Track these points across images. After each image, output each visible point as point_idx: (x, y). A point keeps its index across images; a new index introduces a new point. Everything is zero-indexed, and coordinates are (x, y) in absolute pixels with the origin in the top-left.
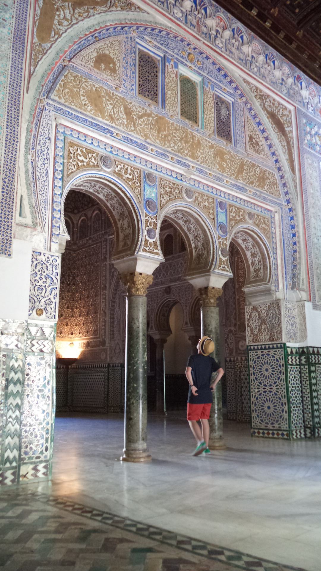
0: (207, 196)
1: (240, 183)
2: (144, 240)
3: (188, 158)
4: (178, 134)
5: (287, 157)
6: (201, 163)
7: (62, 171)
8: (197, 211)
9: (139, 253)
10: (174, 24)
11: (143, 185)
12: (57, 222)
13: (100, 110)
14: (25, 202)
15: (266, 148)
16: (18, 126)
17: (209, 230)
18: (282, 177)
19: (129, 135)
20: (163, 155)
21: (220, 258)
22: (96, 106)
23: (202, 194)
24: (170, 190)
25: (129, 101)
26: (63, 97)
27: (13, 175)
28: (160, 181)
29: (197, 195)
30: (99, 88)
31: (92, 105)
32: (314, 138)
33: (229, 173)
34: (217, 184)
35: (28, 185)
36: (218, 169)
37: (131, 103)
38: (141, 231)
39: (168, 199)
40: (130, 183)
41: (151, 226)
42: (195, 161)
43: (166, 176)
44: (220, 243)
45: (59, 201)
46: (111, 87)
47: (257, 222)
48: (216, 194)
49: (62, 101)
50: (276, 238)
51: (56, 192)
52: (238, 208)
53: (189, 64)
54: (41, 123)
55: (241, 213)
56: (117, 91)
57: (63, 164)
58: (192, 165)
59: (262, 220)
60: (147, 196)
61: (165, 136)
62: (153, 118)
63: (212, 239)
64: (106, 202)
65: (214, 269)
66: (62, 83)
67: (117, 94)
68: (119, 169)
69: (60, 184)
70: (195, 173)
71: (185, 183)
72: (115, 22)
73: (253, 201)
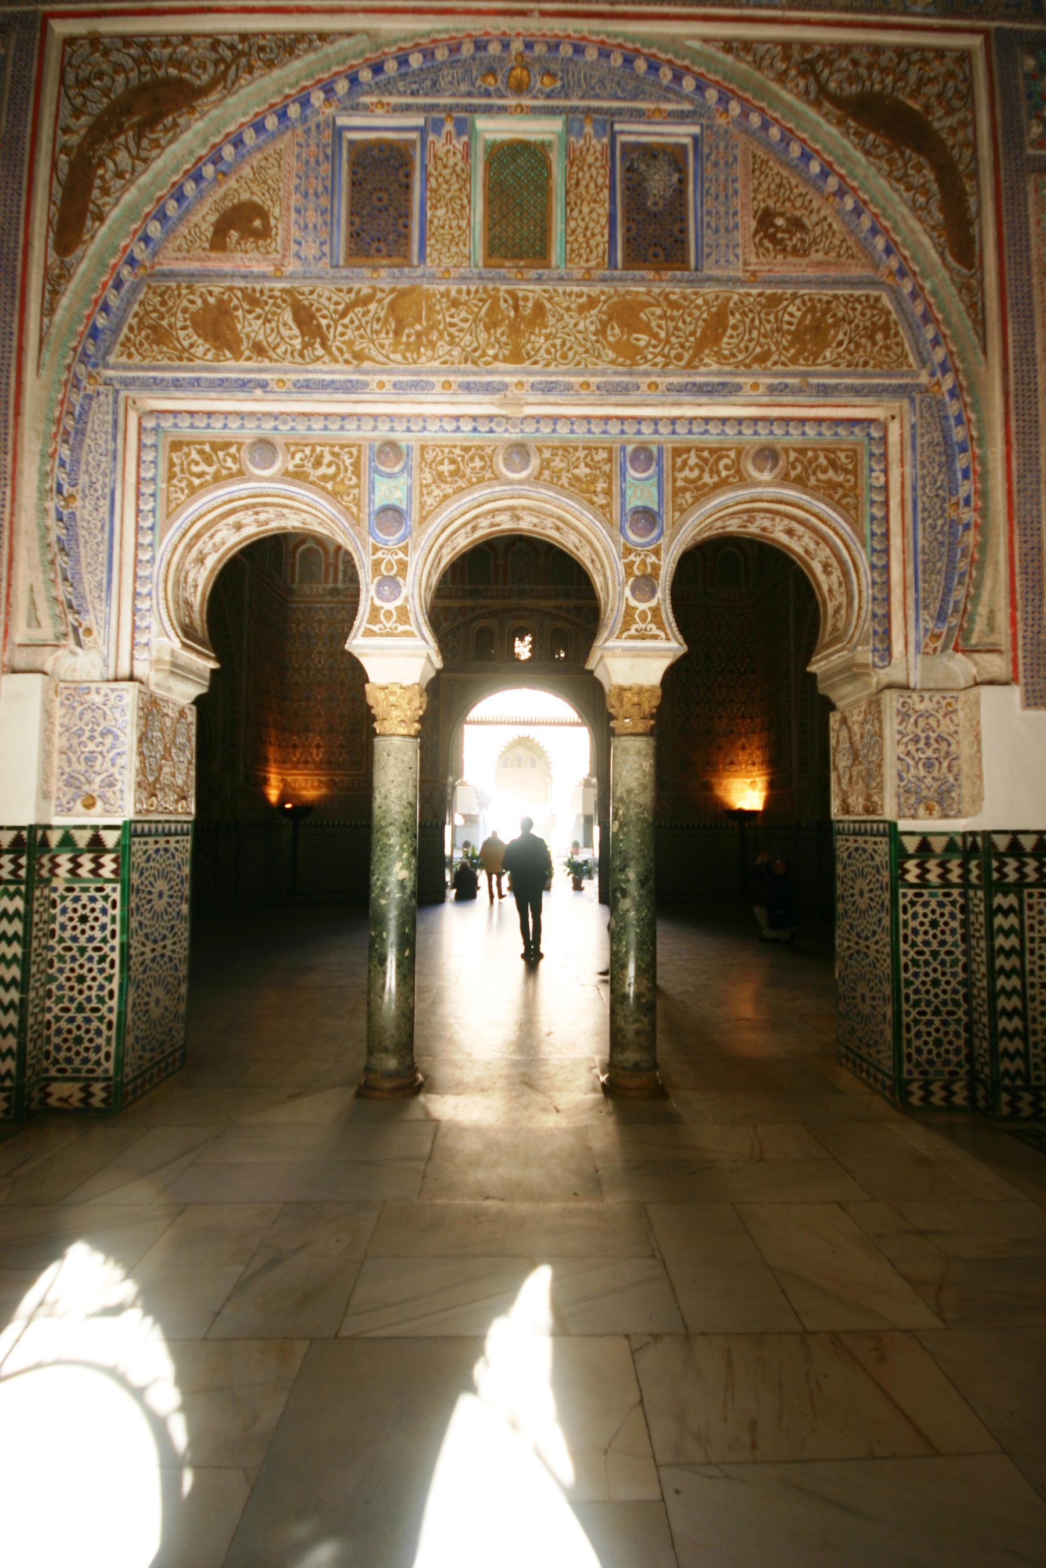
0: (585, 448)
1: (707, 374)
3: (499, 365)
6: (547, 365)
10: (431, 17)
14: (41, 600)
21: (628, 606)
22: (217, 338)
23: (566, 450)
24: (452, 467)
25: (306, 290)
31: (206, 340)
36: (613, 362)
37: (312, 293)
40: (329, 486)
42: (527, 364)
46: (264, 276)
53: (512, 102)
61: (419, 335)
65: (606, 640)
66: (134, 322)
70: (531, 399)
71: (507, 435)
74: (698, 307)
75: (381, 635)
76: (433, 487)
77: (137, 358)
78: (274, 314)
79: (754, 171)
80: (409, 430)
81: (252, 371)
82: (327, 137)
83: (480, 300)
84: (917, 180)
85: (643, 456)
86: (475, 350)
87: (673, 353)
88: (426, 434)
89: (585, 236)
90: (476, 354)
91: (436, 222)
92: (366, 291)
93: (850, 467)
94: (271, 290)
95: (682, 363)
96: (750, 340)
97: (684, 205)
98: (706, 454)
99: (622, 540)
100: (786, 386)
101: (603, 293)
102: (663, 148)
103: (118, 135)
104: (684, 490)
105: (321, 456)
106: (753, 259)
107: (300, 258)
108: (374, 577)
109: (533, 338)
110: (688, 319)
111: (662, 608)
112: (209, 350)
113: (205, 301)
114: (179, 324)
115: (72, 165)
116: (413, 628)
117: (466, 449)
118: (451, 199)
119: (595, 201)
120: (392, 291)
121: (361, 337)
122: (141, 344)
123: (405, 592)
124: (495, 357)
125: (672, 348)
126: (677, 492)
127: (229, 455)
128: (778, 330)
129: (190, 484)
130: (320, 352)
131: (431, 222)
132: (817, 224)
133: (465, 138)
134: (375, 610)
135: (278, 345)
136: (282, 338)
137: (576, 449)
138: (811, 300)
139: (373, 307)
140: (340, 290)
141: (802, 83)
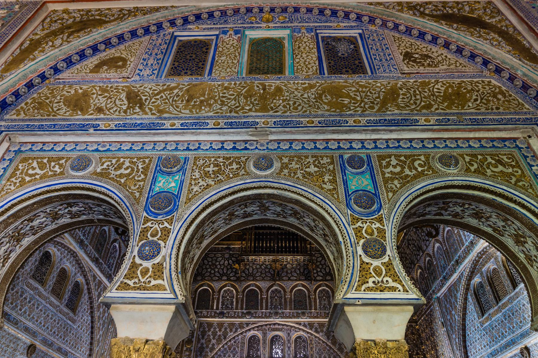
0: (312, 157)
3: (254, 114)
6: (285, 112)
20: (198, 125)
21: (363, 262)
23: (299, 157)
25: (138, 86)
34: (334, 132)
37: (141, 87)
40: (122, 181)
42: (271, 113)
55: (416, 164)
61: (202, 102)
65: (346, 293)
71: (257, 151)
72: (130, 28)
74: (377, 87)
75: (134, 288)
76: (200, 180)
77: (22, 116)
78: (116, 95)
79: (395, 41)
80: (188, 149)
82: (168, 37)
83: (242, 87)
85: (356, 162)
86: (237, 107)
87: (367, 106)
88: (200, 152)
89: (305, 64)
90: (238, 109)
91: (220, 61)
92: (173, 85)
94: (117, 86)
95: (375, 110)
96: (417, 100)
97: (359, 54)
98: (402, 158)
99: (349, 212)
100: (449, 120)
101: (318, 83)
102: (344, 38)
103: (60, 35)
104: (392, 179)
105: (123, 164)
106: (406, 68)
107: (139, 75)
108: (140, 240)
109: (275, 101)
110: (373, 92)
111: (394, 263)
112: (69, 111)
114: (56, 101)
115: (30, 44)
116: (165, 283)
117: (228, 159)
118: (229, 54)
119: (309, 53)
120: (188, 85)
121: (166, 103)
122: (29, 109)
123: (163, 252)
124: (250, 110)
125: (366, 103)
126: (386, 181)
127: (59, 164)
128: (433, 95)
129: (23, 179)
130: (137, 110)
131: (217, 61)
132: (438, 56)
133: (239, 35)
134: (134, 266)
135: (112, 108)
136: (116, 105)
137: (307, 157)
138: (449, 83)
139: (175, 91)
140: (159, 85)
141: (411, 12)
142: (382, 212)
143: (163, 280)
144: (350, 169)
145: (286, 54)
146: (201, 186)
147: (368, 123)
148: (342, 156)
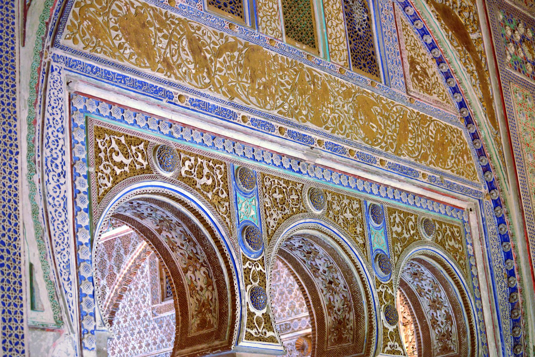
0: (348, 198)
1: (405, 161)
2: (245, 313)
4: (287, 78)
5: (480, 94)
6: (333, 132)
7: (88, 193)
8: (333, 234)
9: (241, 344)
11: (232, 193)
12: (89, 305)
13: (147, 52)
14: (39, 277)
15: (441, 80)
16: (15, 120)
17: (358, 269)
18: (475, 136)
19: (203, 95)
20: (263, 126)
21: (384, 328)
22: (139, 46)
24: (281, 196)
25: (195, 25)
26: (81, 38)
27: (16, 225)
28: (263, 181)
29: (329, 198)
30: (141, 8)
32: (520, 49)
33: (383, 144)
35: (40, 238)
36: (363, 139)
37: (199, 29)
38: (238, 294)
39: (280, 216)
40: (210, 195)
41: (255, 281)
43: (272, 168)
44: (380, 294)
45: (88, 257)
47: (440, 238)
48: (364, 190)
49: (80, 46)
50: (476, 266)
51: (81, 239)
52: (406, 214)
54: (47, 100)
55: (411, 223)
56: (172, 9)
57: (87, 176)
58: (318, 138)
59: (448, 232)
60: (243, 218)
62: (240, 51)
63: (365, 288)
64: (157, 234)
66: (77, 10)
67: (173, 14)
68: (187, 168)
69: (87, 222)
70: (324, 154)
71: (306, 177)
73: (428, 194)
81: (165, 82)
84: (470, 68)
93: (459, 238)
113: (128, 10)
142: (392, 278)
143: (274, 332)
144: (373, 222)
145: (316, 8)
146: (274, 219)
147: (389, 167)
148: (366, 202)
